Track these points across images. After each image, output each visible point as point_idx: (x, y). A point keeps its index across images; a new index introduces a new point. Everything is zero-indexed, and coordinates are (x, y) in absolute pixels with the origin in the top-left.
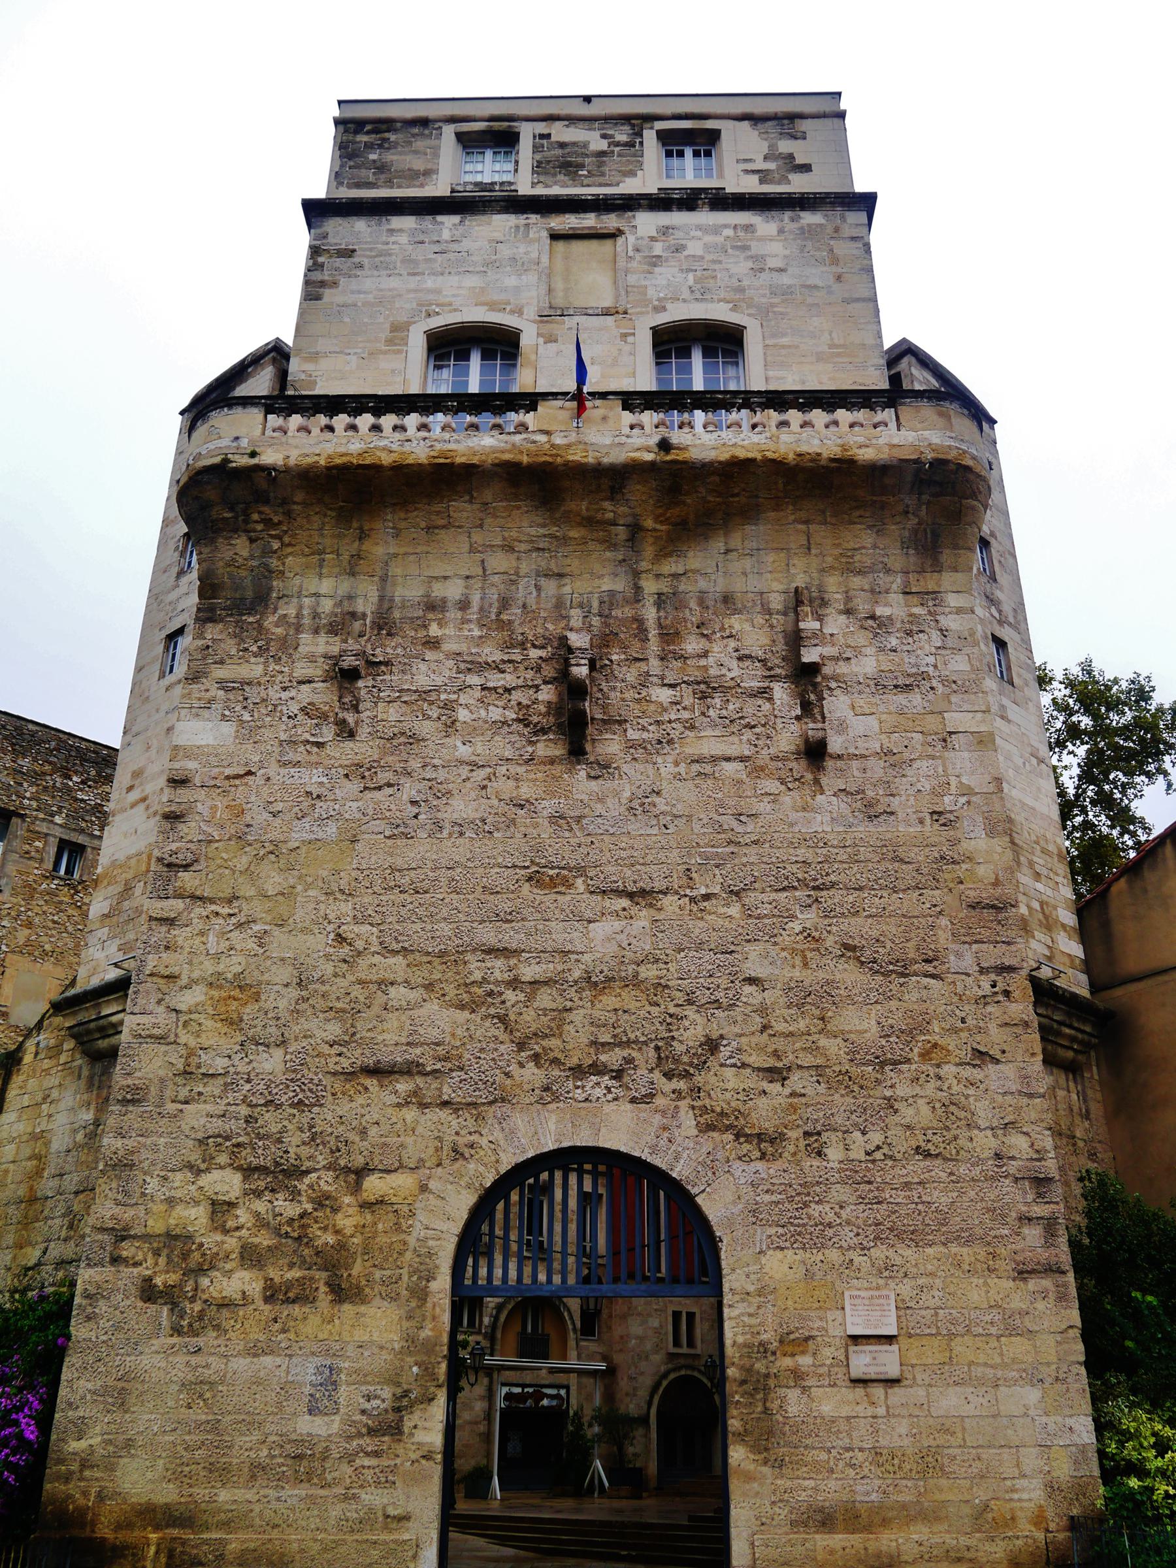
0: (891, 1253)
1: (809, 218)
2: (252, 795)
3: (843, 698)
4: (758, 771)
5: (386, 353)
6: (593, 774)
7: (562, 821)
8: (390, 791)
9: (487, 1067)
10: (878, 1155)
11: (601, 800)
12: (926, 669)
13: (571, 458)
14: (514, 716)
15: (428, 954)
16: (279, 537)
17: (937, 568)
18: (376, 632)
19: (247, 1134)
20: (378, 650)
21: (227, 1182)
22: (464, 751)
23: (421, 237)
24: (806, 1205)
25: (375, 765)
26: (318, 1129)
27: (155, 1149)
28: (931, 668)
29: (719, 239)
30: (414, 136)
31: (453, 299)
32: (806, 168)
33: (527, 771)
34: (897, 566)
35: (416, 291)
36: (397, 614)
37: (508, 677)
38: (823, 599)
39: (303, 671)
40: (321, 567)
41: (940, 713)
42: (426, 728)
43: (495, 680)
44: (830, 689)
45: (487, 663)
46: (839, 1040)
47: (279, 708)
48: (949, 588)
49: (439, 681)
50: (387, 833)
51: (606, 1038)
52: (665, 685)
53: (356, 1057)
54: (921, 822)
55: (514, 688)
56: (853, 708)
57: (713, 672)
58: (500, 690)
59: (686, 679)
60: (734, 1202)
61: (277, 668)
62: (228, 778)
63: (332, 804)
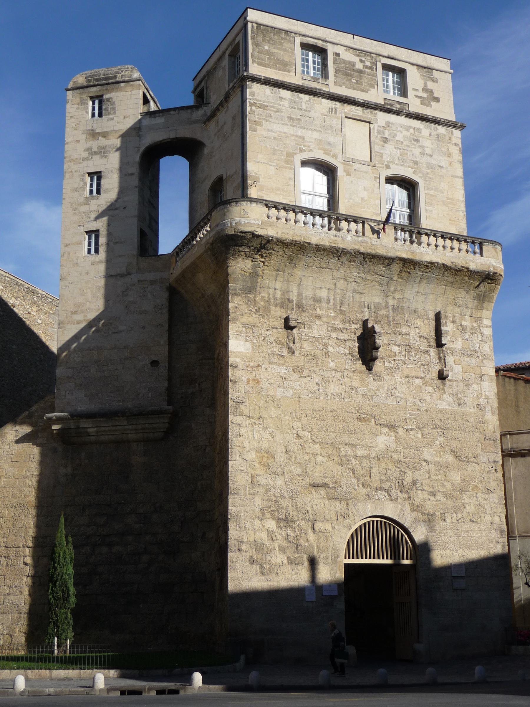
0: (463, 552)
1: (441, 130)
2: (261, 374)
3: (452, 357)
4: (426, 383)
5: (286, 168)
6: (375, 378)
7: (366, 397)
8: (309, 378)
9: (349, 487)
10: (460, 521)
11: (378, 390)
12: (476, 349)
14: (348, 352)
16: (263, 262)
17: (482, 308)
18: (298, 309)
19: (276, 507)
20: (300, 317)
21: (272, 524)
22: (332, 364)
24: (441, 536)
25: (303, 367)
26: (299, 506)
27: (246, 511)
28: (478, 349)
29: (408, 134)
30: (282, 39)
31: (310, 144)
32: (437, 100)
33: (354, 375)
35: (294, 135)
37: (346, 335)
38: (446, 315)
39: (273, 323)
40: (277, 277)
41: (480, 367)
42: (319, 353)
43: (342, 336)
44: (447, 353)
45: (338, 329)
46: (450, 483)
47: (266, 339)
48: (484, 317)
50: (310, 396)
51: (383, 478)
52: (396, 345)
53: (307, 481)
54: (474, 407)
55: (347, 340)
57: (412, 342)
58: (343, 341)
59: (403, 343)
60: (422, 535)
61: (263, 320)
62: (252, 367)
63: (290, 382)
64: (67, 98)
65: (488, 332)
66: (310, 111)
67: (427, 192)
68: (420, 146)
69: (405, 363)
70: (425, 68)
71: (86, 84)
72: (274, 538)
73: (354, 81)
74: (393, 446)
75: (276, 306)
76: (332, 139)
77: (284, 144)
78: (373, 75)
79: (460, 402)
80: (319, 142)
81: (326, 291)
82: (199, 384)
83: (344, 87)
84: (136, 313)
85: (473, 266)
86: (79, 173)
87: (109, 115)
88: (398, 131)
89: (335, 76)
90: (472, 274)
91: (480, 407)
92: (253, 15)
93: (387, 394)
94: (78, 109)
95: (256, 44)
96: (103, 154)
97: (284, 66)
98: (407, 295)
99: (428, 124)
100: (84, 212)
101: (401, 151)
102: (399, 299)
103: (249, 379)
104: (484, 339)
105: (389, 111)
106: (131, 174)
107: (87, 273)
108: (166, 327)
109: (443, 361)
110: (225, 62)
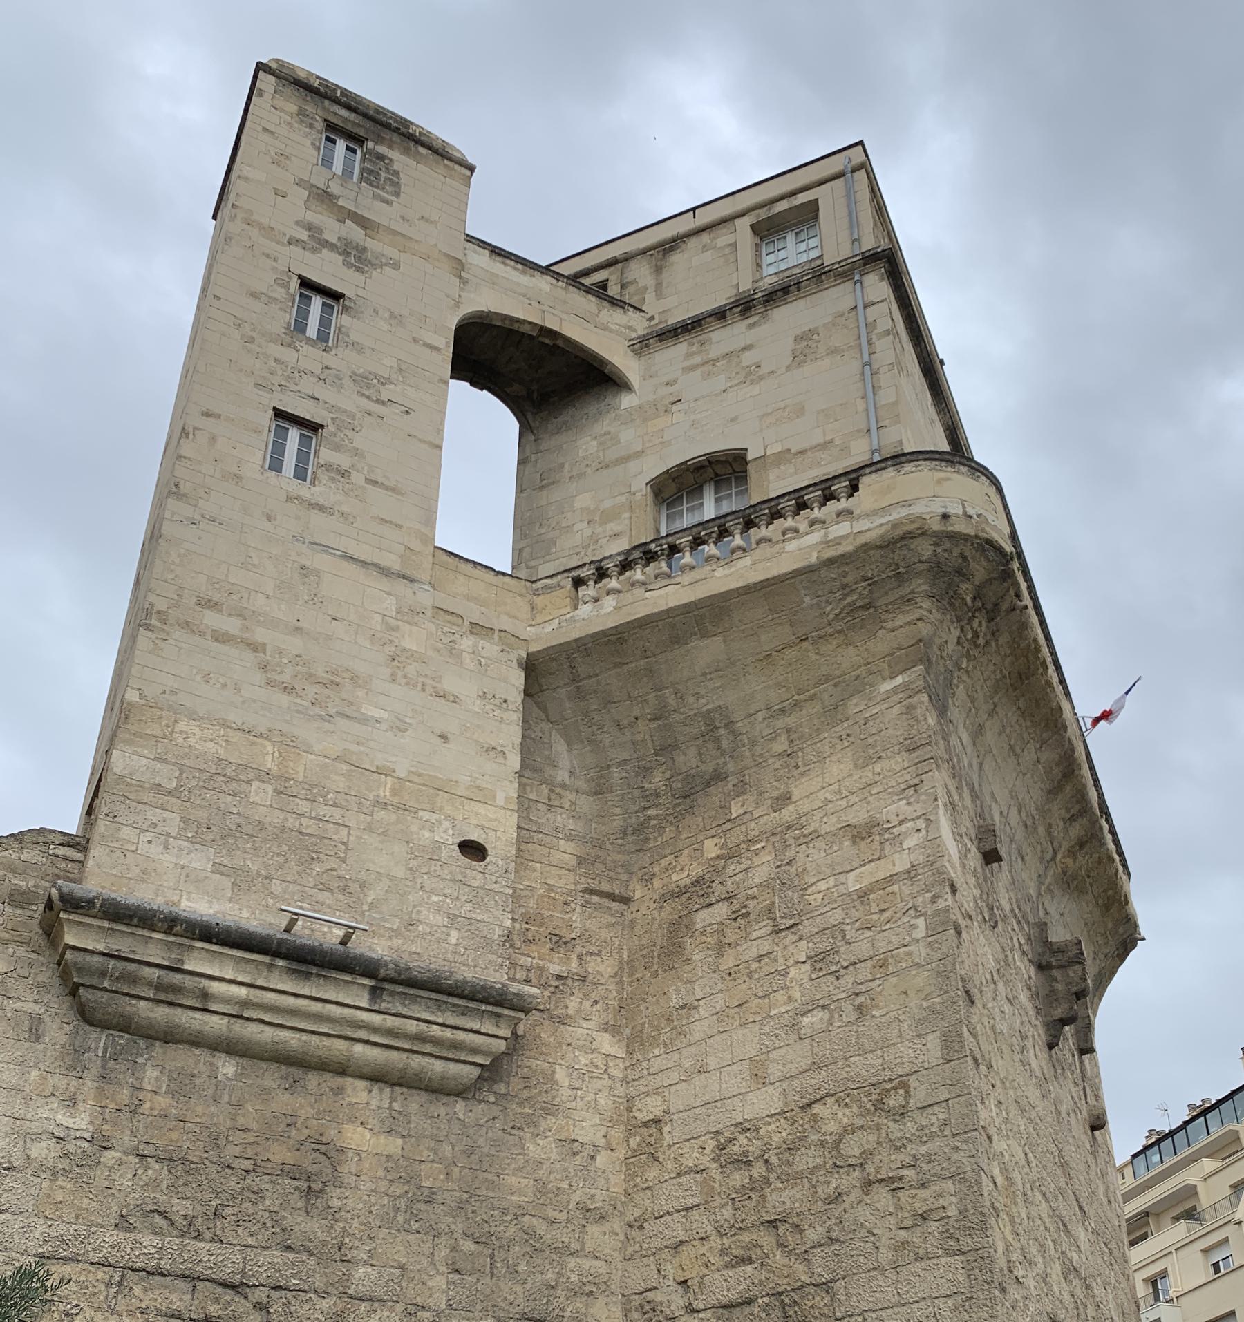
82: (580, 957)
84: (423, 690)
87: (378, 187)
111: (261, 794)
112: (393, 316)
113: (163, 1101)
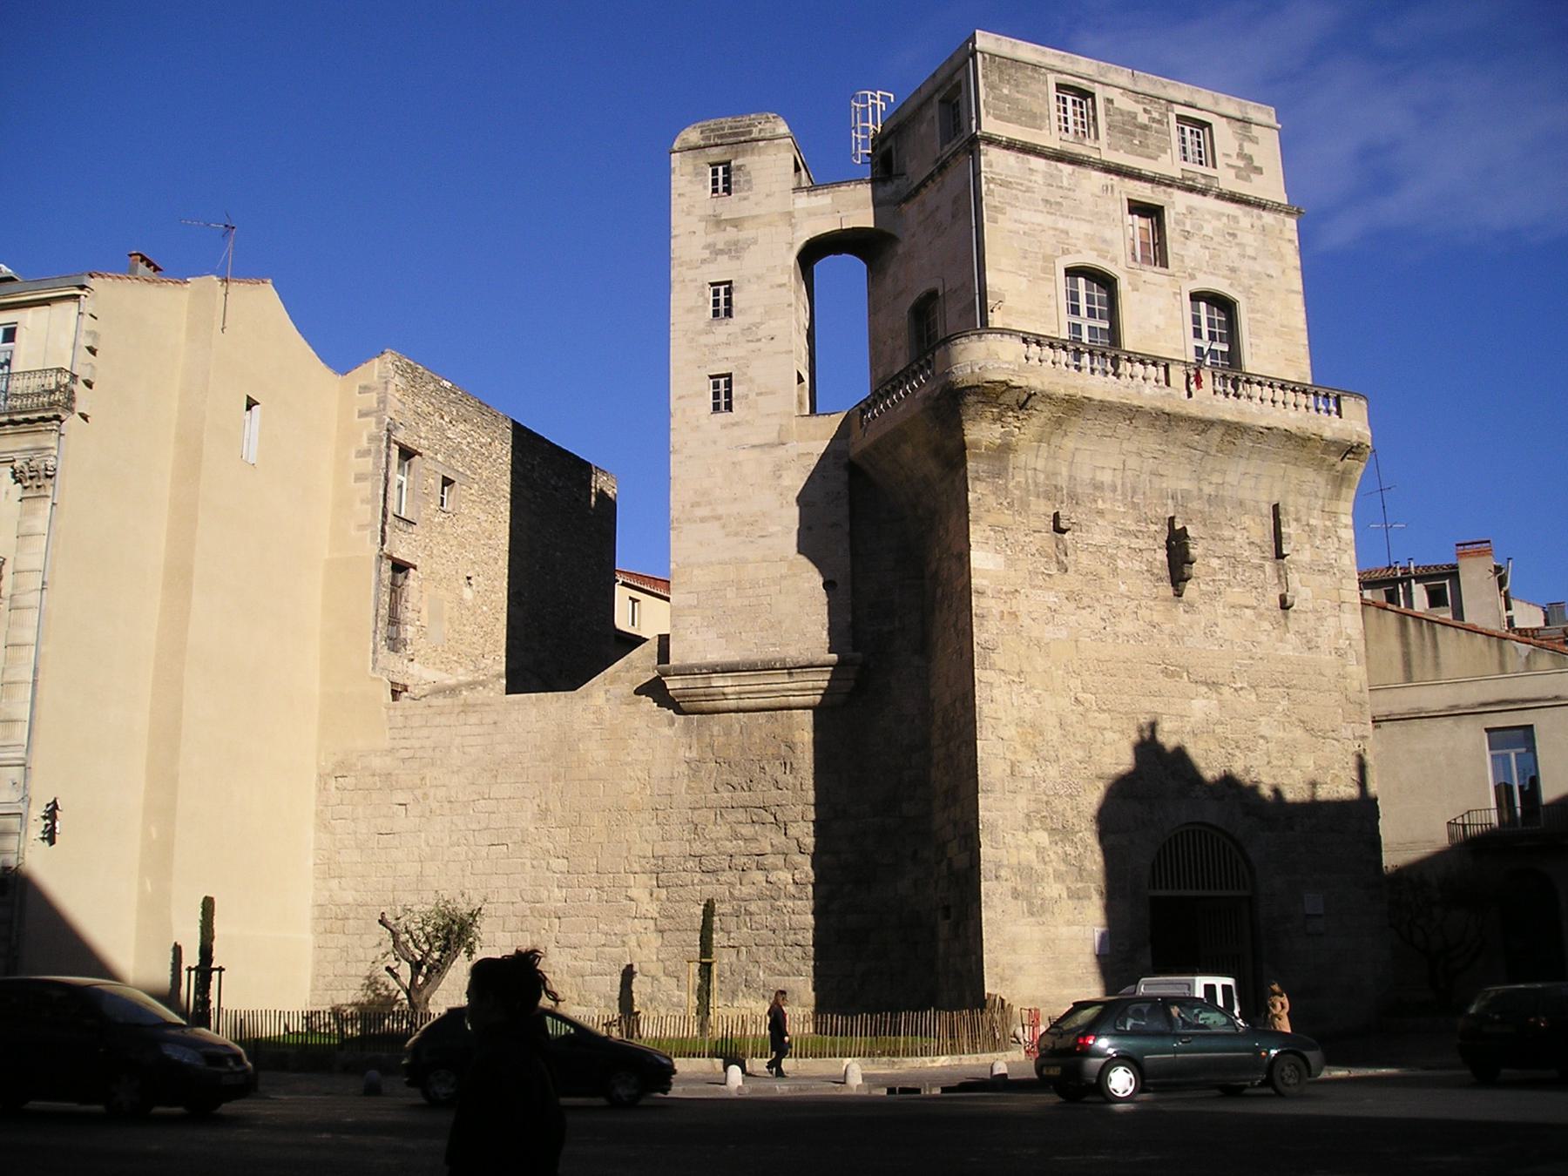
1: (1268, 218)
2: (1021, 605)
3: (1296, 575)
4: (1260, 616)
5: (1043, 279)
8: (1089, 610)
11: (1191, 627)
13: (1190, 410)
15: (1120, 713)
16: (1019, 428)
20: (1073, 515)
21: (1042, 837)
22: (1123, 588)
23: (1049, 182)
27: (1005, 818)
29: (1219, 224)
32: (1259, 170)
34: (1321, 493)
36: (1079, 490)
37: (1141, 542)
40: (1038, 450)
42: (1103, 571)
49: (1107, 539)
54: (1330, 653)
56: (1301, 582)
62: (1006, 593)
64: (673, 165)
65: (1348, 535)
66: (1074, 191)
67: (1251, 316)
68: (1238, 244)
69: (1229, 585)
70: (1239, 120)
71: (702, 143)
72: (1047, 859)
73: (1137, 143)
74: (1216, 715)
75: (1038, 496)
76: (1108, 234)
77: (1039, 241)
78: (1163, 133)
79: (1311, 647)
80: (1090, 238)
81: (1110, 472)
83: (1122, 151)
85: (1328, 434)
86: (695, 284)
88: (1205, 220)
89: (1108, 134)
90: (1329, 445)
91: (1340, 653)
92: (985, 41)
93: (1205, 633)
94: (691, 182)
95: (991, 87)
96: (733, 254)
97: (1034, 119)
98: (1228, 479)
99: (1248, 209)
100: (706, 346)
101: (1212, 251)
102: (1217, 484)
103: (1002, 612)
104: (1343, 546)
105: (1191, 189)
106: (780, 286)
107: (715, 442)
108: (847, 527)
109: (1284, 580)
110: (934, 111)
111: (730, 593)
112: (758, 277)
113: (722, 739)
